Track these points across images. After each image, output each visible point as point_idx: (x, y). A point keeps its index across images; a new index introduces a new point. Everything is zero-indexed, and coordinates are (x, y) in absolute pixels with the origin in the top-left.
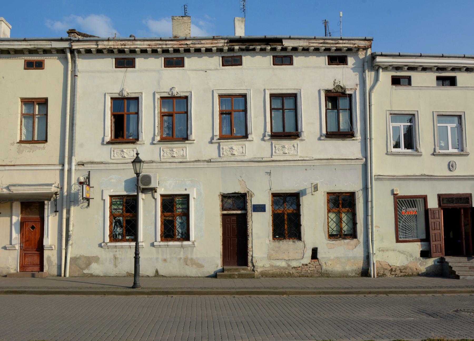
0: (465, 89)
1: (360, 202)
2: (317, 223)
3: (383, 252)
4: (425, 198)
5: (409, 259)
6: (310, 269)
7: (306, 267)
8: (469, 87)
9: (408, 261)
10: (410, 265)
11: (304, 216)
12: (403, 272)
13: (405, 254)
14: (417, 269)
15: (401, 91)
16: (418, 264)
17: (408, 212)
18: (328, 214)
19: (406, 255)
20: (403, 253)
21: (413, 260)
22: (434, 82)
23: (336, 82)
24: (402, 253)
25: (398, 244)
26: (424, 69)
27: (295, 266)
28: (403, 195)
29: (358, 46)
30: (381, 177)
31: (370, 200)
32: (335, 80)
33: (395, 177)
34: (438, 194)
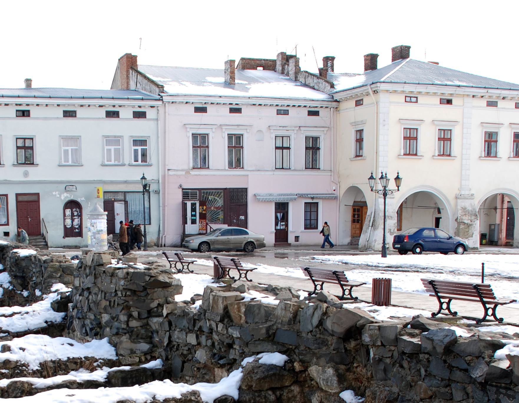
22: (14, 115)
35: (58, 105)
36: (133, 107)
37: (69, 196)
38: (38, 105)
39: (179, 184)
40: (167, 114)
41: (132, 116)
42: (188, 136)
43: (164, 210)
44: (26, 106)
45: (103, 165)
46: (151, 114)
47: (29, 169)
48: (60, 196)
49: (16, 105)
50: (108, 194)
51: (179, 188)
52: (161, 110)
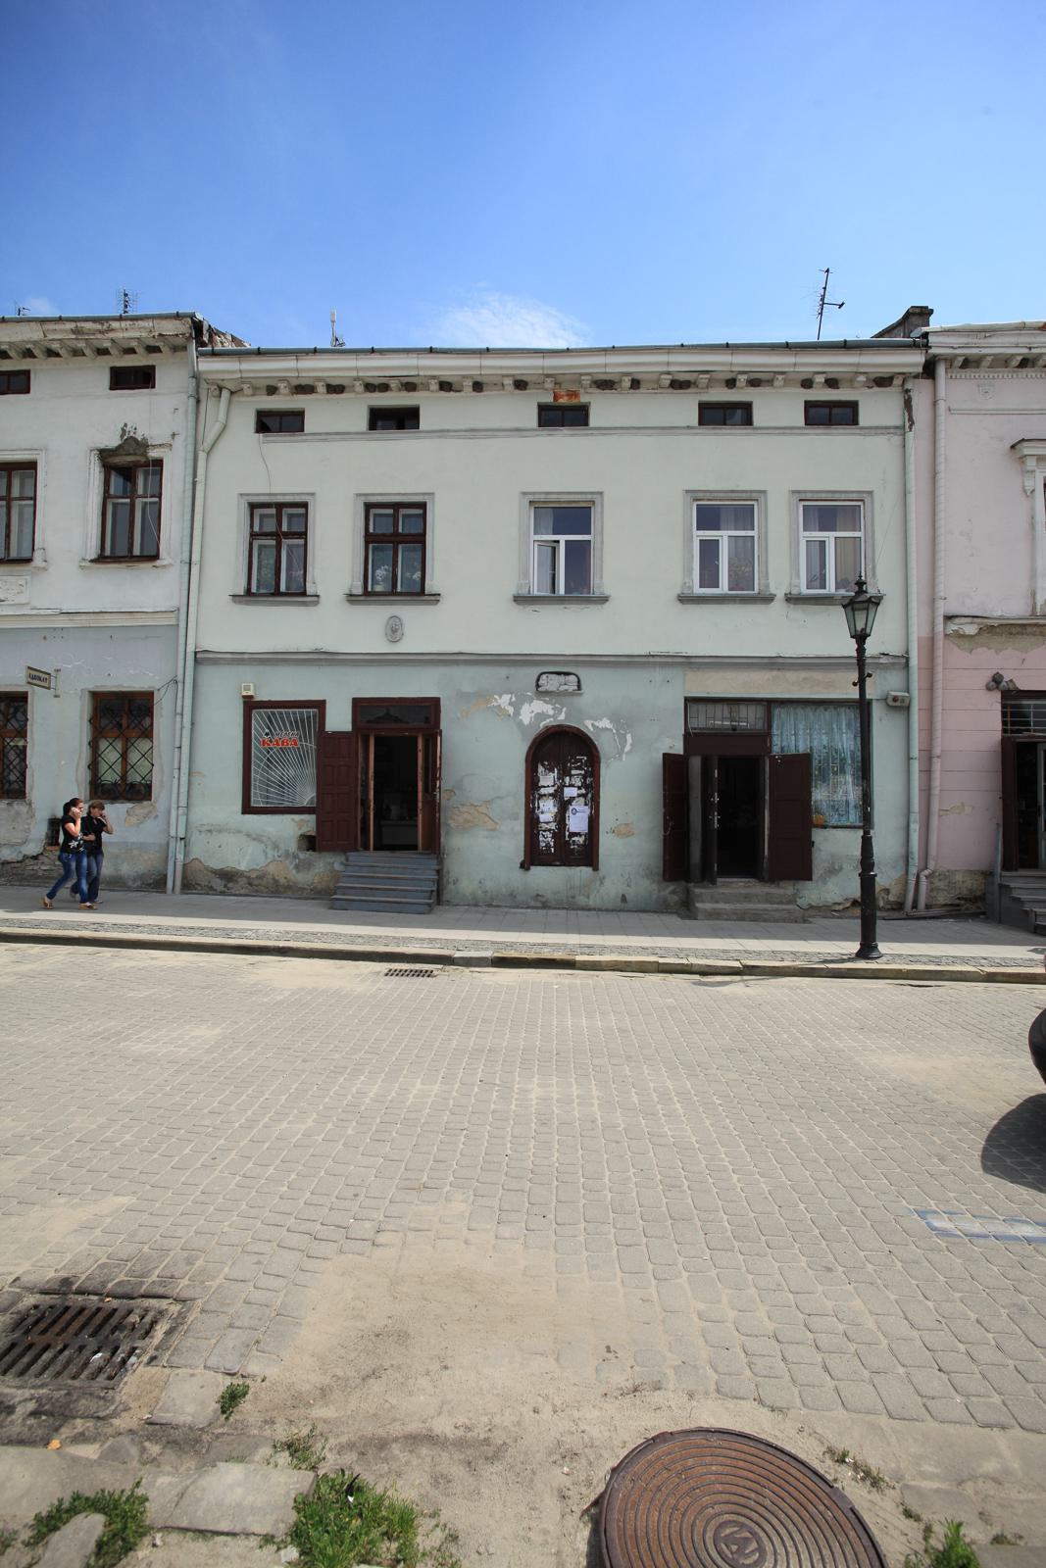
0: (440, 437)
1: (162, 716)
2: (63, 762)
3: (209, 834)
4: (320, 705)
5: (270, 855)
6: (44, 868)
7: (32, 862)
8: (448, 431)
9: (266, 857)
10: (271, 869)
11: (33, 744)
12: (256, 886)
13: (262, 842)
14: (289, 877)
15: (281, 448)
16: (291, 867)
17: (276, 741)
18: (94, 745)
19: (263, 845)
20: (257, 839)
21: (279, 857)
22: (363, 423)
23: (127, 430)
24: (254, 839)
25: (247, 816)
26: (335, 389)
27: (9, 859)
28: (266, 698)
29: (160, 335)
30: (211, 656)
31: (179, 710)
32: (126, 425)
33: (246, 656)
34: (354, 699)
35: (520, 385)
36: (807, 384)
37: (551, 712)
38: (446, 386)
39: (989, 674)
40: (942, 406)
41: (801, 422)
42: (1029, 488)
43: (927, 771)
44: (405, 394)
45: (685, 599)
46: (879, 409)
47: (411, 615)
48: (517, 713)
49: (370, 387)
50: (702, 707)
51: (989, 688)
52: (921, 393)
